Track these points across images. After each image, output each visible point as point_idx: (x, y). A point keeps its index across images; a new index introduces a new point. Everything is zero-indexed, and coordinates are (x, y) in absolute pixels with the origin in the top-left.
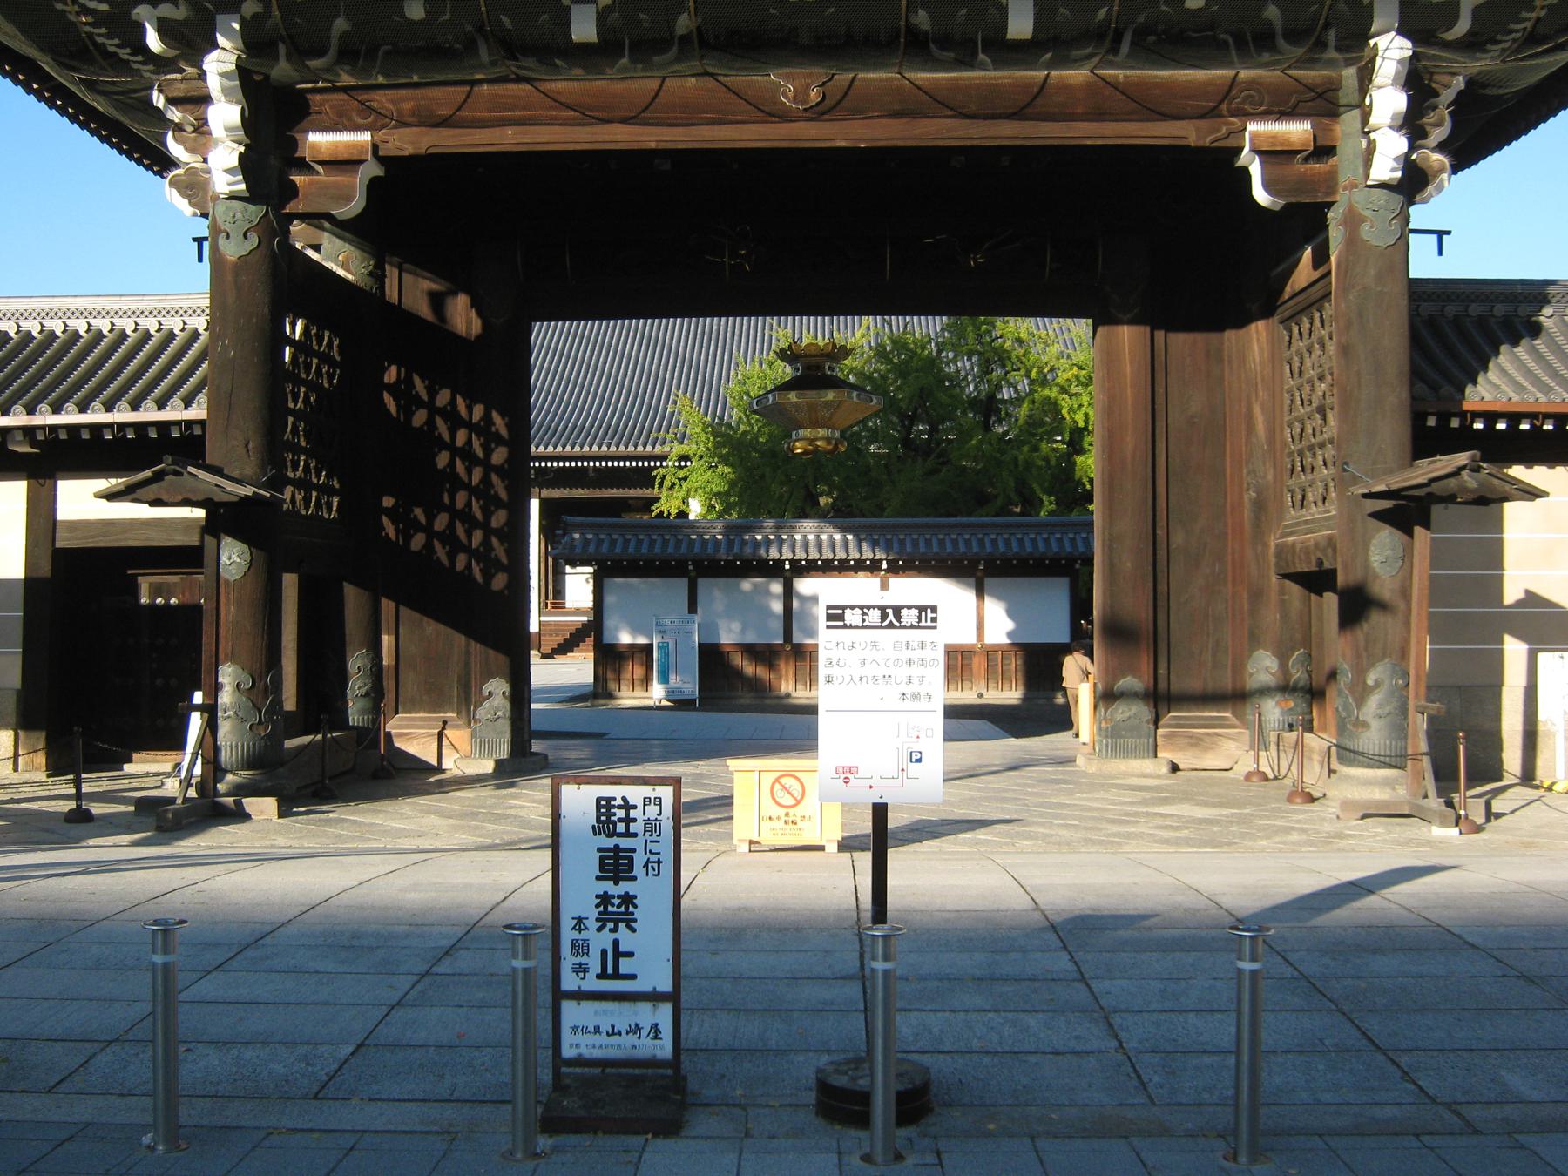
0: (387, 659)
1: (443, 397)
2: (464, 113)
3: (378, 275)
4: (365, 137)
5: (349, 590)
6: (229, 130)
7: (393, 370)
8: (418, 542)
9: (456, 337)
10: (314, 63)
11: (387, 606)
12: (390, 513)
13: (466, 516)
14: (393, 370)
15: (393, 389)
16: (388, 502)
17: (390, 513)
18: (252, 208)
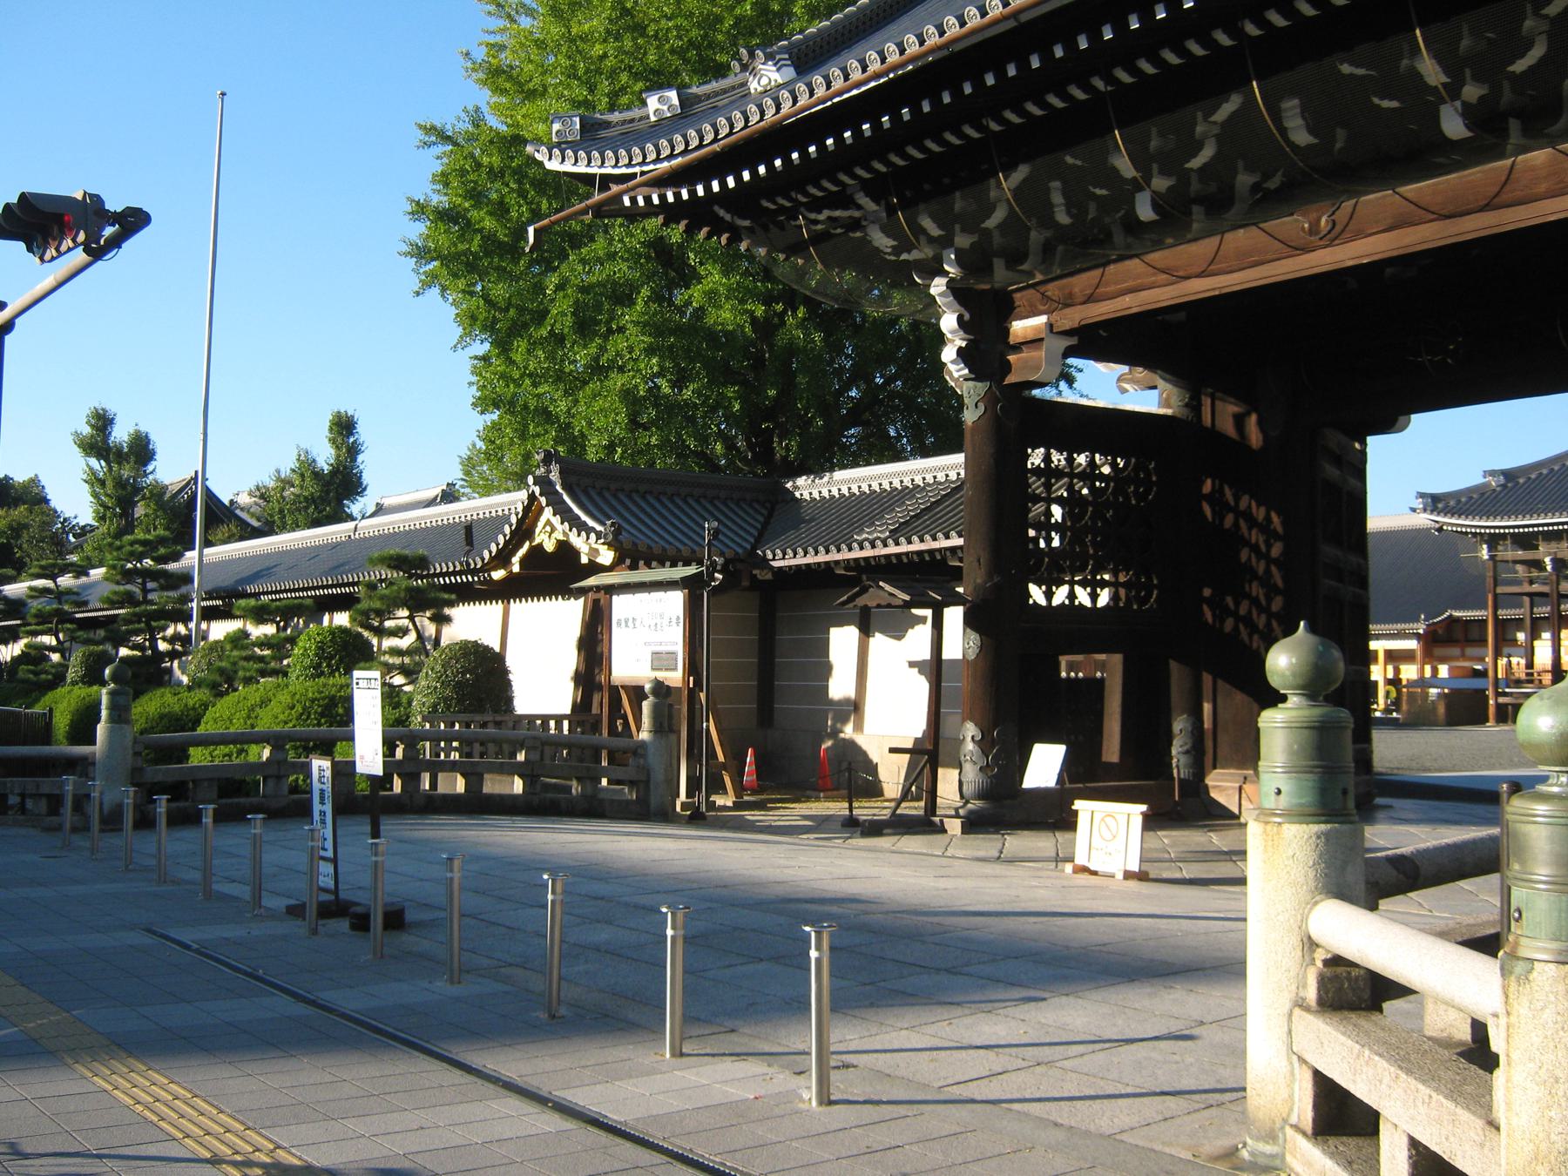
0: (1207, 724)
1: (1244, 502)
2: (1101, 290)
3: (1194, 405)
4: (1042, 320)
5: (1173, 665)
6: (952, 332)
7: (1209, 482)
8: (1229, 624)
9: (1249, 447)
10: (1025, 267)
11: (1207, 679)
12: (1209, 601)
13: (1255, 601)
14: (1209, 482)
15: (1209, 498)
16: (1207, 592)
17: (1209, 601)
18: (979, 384)
